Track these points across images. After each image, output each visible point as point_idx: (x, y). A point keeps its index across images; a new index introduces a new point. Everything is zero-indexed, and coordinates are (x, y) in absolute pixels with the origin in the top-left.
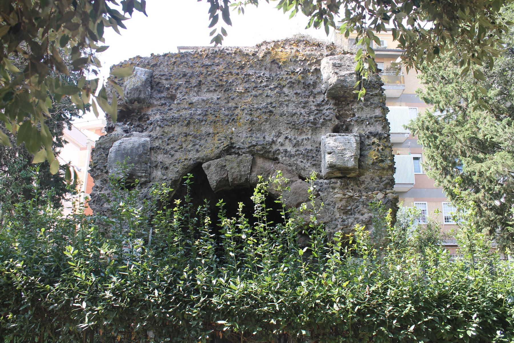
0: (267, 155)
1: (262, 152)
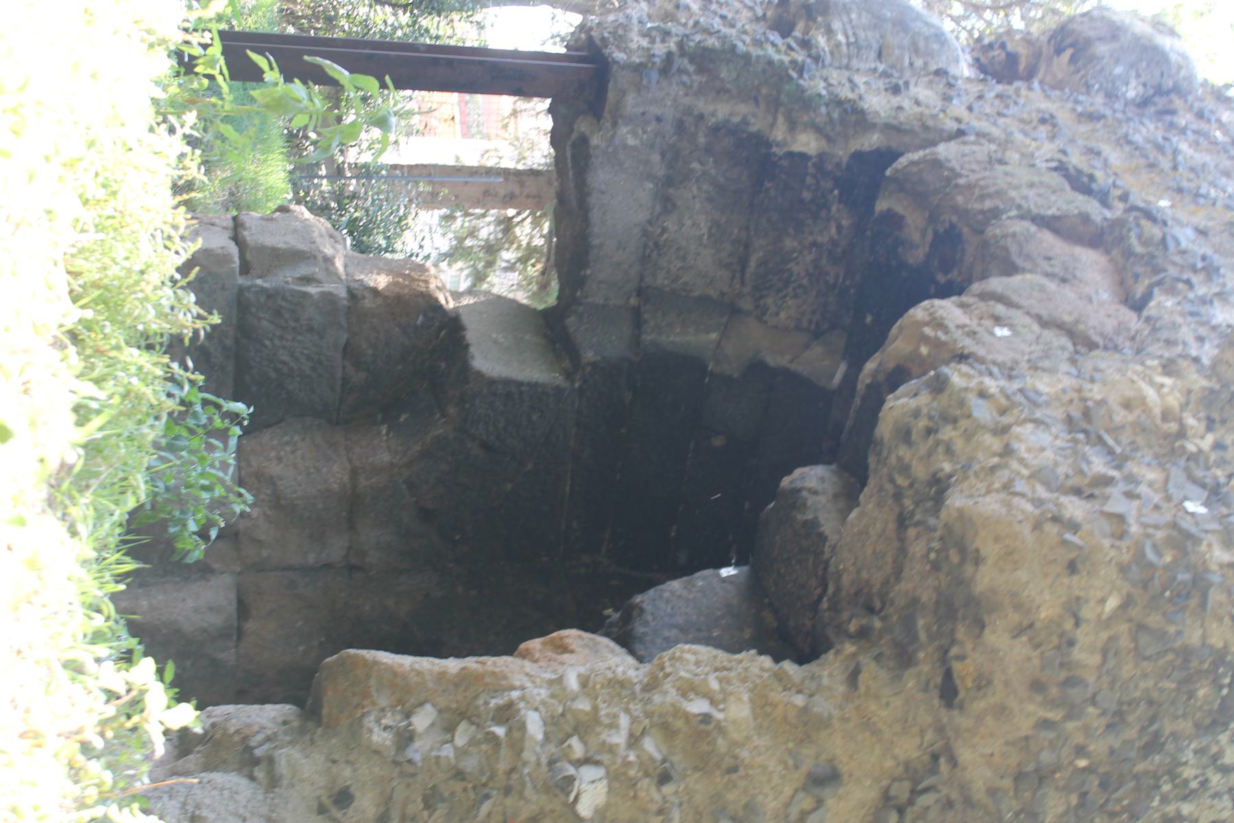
0: (1139, 269)
1: (1139, 249)
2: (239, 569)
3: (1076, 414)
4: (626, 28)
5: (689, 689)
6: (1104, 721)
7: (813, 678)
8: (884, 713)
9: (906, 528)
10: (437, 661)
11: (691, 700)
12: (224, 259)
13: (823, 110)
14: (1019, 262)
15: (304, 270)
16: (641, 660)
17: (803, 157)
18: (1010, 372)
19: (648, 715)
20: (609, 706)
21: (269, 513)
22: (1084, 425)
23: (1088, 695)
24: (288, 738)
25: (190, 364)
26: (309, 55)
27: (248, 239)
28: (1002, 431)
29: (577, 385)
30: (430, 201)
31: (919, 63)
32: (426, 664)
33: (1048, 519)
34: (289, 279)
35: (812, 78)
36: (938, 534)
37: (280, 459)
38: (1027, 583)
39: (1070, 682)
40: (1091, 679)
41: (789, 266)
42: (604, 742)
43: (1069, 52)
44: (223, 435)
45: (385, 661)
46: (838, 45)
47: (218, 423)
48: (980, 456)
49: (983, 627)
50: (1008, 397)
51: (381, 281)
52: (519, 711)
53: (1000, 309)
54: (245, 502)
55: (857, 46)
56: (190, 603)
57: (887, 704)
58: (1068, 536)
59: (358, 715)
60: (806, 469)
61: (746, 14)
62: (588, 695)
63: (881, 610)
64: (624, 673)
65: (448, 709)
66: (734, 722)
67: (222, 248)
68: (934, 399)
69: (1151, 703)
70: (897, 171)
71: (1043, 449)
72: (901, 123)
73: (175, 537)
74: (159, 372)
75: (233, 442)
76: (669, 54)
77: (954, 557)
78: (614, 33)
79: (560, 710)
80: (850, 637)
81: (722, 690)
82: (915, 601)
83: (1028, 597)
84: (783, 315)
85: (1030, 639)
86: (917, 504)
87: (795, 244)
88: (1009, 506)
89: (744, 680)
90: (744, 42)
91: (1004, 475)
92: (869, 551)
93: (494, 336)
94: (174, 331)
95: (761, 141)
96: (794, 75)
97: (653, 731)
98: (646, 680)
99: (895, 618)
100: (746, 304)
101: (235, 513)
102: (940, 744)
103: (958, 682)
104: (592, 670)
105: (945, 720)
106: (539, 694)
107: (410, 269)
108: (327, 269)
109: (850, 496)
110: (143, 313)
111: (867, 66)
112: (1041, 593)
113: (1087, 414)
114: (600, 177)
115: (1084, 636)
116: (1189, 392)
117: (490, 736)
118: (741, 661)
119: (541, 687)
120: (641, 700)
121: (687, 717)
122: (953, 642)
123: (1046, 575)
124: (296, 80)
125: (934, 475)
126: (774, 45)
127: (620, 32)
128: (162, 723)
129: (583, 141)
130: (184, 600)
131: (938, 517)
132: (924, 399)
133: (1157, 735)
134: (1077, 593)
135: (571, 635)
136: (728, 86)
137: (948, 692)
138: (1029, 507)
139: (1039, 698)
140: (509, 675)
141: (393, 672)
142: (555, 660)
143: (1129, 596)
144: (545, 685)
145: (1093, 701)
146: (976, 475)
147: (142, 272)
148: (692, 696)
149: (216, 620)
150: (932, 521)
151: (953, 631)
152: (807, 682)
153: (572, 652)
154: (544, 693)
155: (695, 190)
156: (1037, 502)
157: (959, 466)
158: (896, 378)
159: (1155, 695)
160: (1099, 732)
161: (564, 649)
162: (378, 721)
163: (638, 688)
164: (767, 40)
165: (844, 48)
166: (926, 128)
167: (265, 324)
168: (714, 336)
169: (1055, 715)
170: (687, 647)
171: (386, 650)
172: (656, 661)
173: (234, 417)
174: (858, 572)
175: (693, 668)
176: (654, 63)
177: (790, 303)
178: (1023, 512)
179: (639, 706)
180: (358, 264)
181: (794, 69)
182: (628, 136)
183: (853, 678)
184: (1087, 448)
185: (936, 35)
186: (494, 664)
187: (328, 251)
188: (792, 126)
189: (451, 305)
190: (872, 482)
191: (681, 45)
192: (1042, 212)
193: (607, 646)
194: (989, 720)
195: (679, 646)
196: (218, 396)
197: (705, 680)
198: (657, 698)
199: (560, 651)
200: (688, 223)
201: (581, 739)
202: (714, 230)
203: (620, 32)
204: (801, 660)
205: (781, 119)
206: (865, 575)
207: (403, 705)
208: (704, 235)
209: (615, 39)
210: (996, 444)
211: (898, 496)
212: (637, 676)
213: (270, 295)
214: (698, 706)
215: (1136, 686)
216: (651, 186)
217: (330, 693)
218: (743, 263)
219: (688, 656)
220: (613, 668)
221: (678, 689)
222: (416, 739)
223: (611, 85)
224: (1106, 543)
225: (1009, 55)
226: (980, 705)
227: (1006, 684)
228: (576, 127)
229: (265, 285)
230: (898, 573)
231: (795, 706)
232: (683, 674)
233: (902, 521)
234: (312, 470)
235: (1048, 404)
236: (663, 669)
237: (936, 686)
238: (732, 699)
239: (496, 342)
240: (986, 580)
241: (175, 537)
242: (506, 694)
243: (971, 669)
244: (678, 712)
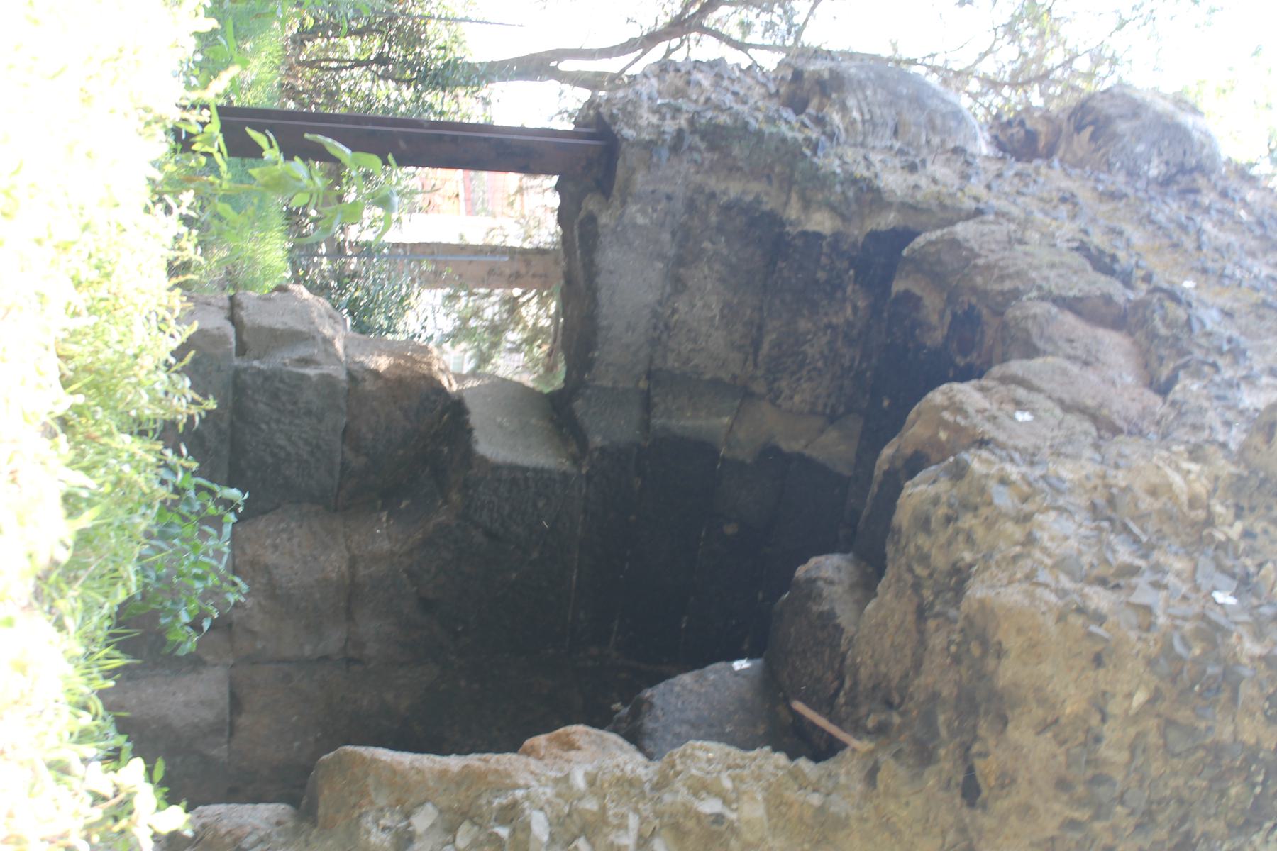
0: (1164, 352)
1: (1163, 331)
2: (231, 662)
3: (1100, 501)
4: (636, 104)
5: (701, 788)
6: (1132, 821)
7: (829, 775)
8: (904, 813)
9: (925, 619)
10: (438, 758)
11: (703, 799)
12: (220, 339)
13: (838, 188)
14: (1041, 344)
15: (302, 351)
16: (650, 757)
17: (818, 236)
18: (1032, 458)
19: (658, 815)
20: (616, 806)
21: (263, 602)
22: (1109, 513)
23: (1117, 794)
24: (282, 840)
25: (184, 451)
26: (310, 133)
27: (245, 319)
28: (1025, 518)
29: (584, 471)
30: (433, 281)
31: (936, 140)
32: (427, 761)
33: (1073, 611)
34: (287, 361)
35: (826, 156)
36: (958, 626)
37: (275, 547)
38: (1052, 677)
39: (1097, 780)
40: (1119, 777)
41: (803, 348)
42: (612, 844)
43: (1089, 130)
44: (217, 522)
45: (384, 758)
46: (853, 122)
47: (212, 509)
48: (1002, 545)
49: (1005, 723)
50: (1029, 484)
51: (382, 363)
52: (523, 811)
53: (1021, 393)
54: (239, 592)
55: (872, 124)
56: (181, 697)
57: (907, 804)
58: (1094, 628)
59: (356, 815)
60: (822, 559)
61: (758, 90)
62: (596, 794)
63: (900, 705)
64: (633, 771)
65: (450, 809)
66: (748, 822)
67: (218, 328)
68: (954, 486)
69: (1181, 801)
70: (914, 251)
71: (1066, 538)
72: (918, 202)
73: (166, 629)
74: (152, 459)
75: (227, 530)
76: (680, 132)
77: (976, 650)
78: (623, 110)
79: (566, 810)
80: (868, 733)
81: (735, 789)
82: (934, 697)
83: (1053, 691)
84: (797, 398)
85: (1055, 736)
86: (937, 594)
87: (810, 325)
88: (1032, 597)
89: (758, 778)
90: (757, 120)
91: (1025, 565)
92: (887, 643)
93: (499, 420)
94: (167, 417)
95: (774, 220)
96: (808, 152)
97: (663, 831)
98: (655, 779)
99: (915, 713)
100: (759, 387)
101: (229, 603)
102: (963, 844)
103: (980, 780)
104: (600, 768)
105: (967, 820)
106: (544, 793)
107: (412, 351)
108: (326, 350)
109: (868, 583)
110: (136, 398)
111: (883, 144)
112: (1066, 687)
113: (1111, 501)
114: (609, 256)
115: (1111, 732)
116: (1217, 478)
117: (493, 837)
118: (755, 759)
119: (546, 786)
120: (652, 799)
121: (699, 817)
122: (975, 738)
123: (1071, 669)
124: (297, 159)
125: (954, 564)
126: (787, 122)
127: (630, 108)
128: (150, 827)
129: (592, 219)
130: (174, 694)
131: (958, 609)
132: (943, 486)
133: (1188, 835)
134: (1103, 687)
135: (578, 731)
136: (740, 164)
137: (971, 791)
138: (1052, 598)
139: (1065, 797)
140: (513, 773)
141: (393, 770)
142: (561, 757)
143: (1157, 689)
144: (550, 783)
145: (1121, 800)
146: (998, 565)
147: (136, 356)
148: (704, 795)
149: (208, 715)
150: (952, 612)
151: (975, 727)
152: (823, 779)
153: (579, 749)
154: (549, 792)
155: (706, 271)
156: (1062, 593)
157: (979, 556)
158: (914, 464)
159: (1186, 794)
160: (1127, 833)
161: (570, 745)
162: (376, 821)
163: (647, 787)
164: (780, 117)
165: (859, 126)
166: (943, 207)
167: (261, 406)
168: (726, 420)
169: (1081, 815)
170: (699, 743)
171: (385, 746)
172: (666, 758)
173: (229, 504)
174: (876, 665)
175: (704, 765)
176: (664, 141)
177: (805, 386)
178: (1046, 603)
179: (648, 806)
180: (359, 345)
181: (808, 146)
182: (637, 214)
183: (871, 776)
184: (1112, 537)
185: (953, 113)
186: (498, 761)
187: (327, 331)
188: (807, 204)
189: (455, 387)
190: (890, 572)
191: (691, 122)
192: (1064, 293)
193: (615, 743)
194: (1013, 820)
195: (691, 742)
196: (212, 481)
197: (718, 778)
198: (668, 798)
199: (566, 748)
200: (699, 304)
201: (588, 840)
202: (726, 312)
203: (630, 108)
204: (817, 757)
205: (794, 197)
206: (883, 669)
207: (403, 805)
208: (715, 316)
209: (624, 116)
210: (1018, 532)
211: (917, 586)
212: (646, 774)
213: (268, 377)
214: (710, 806)
215: (1166, 784)
216: (660, 265)
217: (326, 792)
218: (756, 344)
219: (700, 753)
220: (622, 765)
221: (689, 788)
222: (416, 840)
223: (620, 163)
224: (1133, 635)
225: (1028, 133)
226: (1003, 805)
227: (1031, 782)
228: (583, 205)
229: (262, 367)
230: (917, 666)
231: (811, 806)
232: (694, 772)
233: (922, 613)
234: (309, 559)
235: (1071, 491)
236: (673, 766)
237: (957, 785)
238: (745, 798)
239: (500, 426)
240: (1009, 674)
241: (166, 629)
242: (510, 793)
243: (994, 766)
244: (689, 812)
